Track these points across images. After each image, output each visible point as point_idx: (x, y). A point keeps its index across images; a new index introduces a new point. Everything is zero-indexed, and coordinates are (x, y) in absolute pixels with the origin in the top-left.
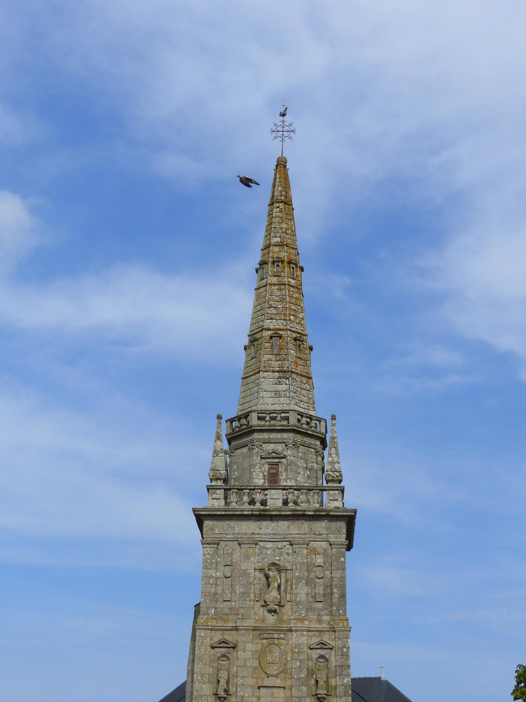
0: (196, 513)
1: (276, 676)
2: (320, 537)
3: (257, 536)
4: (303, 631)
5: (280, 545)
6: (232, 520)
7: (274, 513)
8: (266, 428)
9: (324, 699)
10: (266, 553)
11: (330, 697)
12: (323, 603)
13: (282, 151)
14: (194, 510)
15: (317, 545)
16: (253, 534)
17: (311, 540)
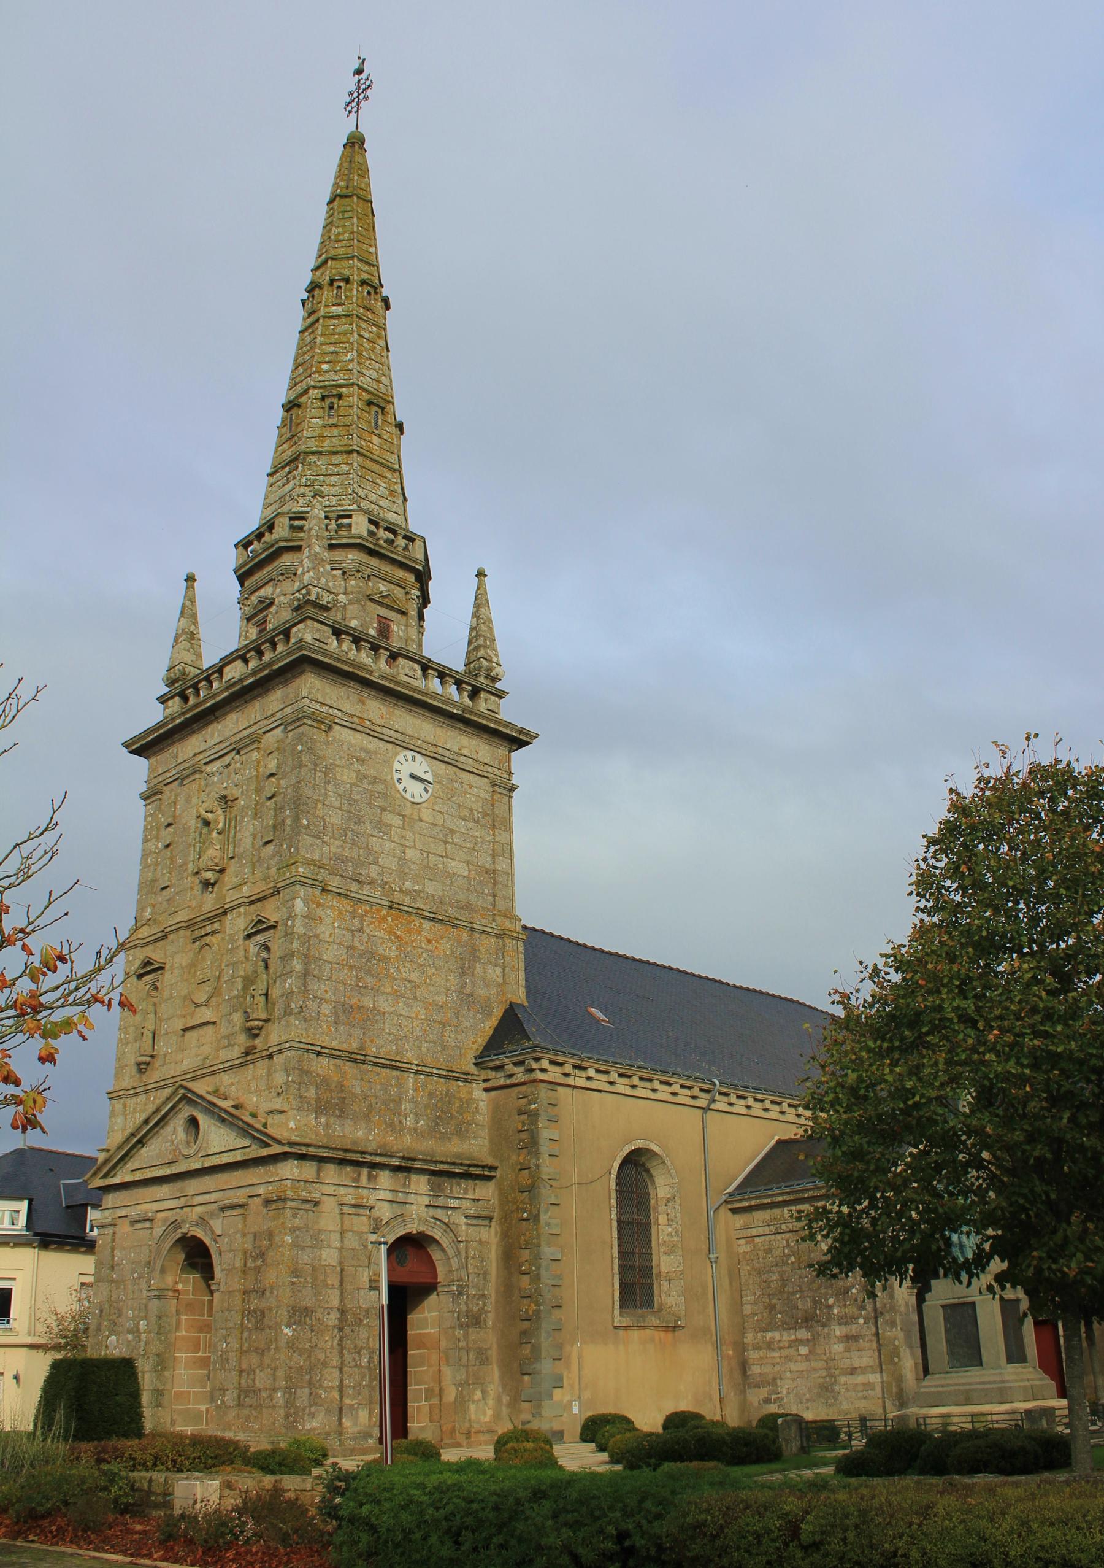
0: (130, 749)
1: (206, 1004)
2: (273, 719)
3: (201, 757)
4: (239, 906)
5: (227, 759)
6: (174, 743)
7: (208, 704)
8: (250, 565)
9: (260, 1029)
10: (213, 782)
11: (270, 1024)
12: (274, 843)
13: (357, 125)
14: (126, 745)
15: (273, 736)
16: (195, 755)
17: (263, 730)
